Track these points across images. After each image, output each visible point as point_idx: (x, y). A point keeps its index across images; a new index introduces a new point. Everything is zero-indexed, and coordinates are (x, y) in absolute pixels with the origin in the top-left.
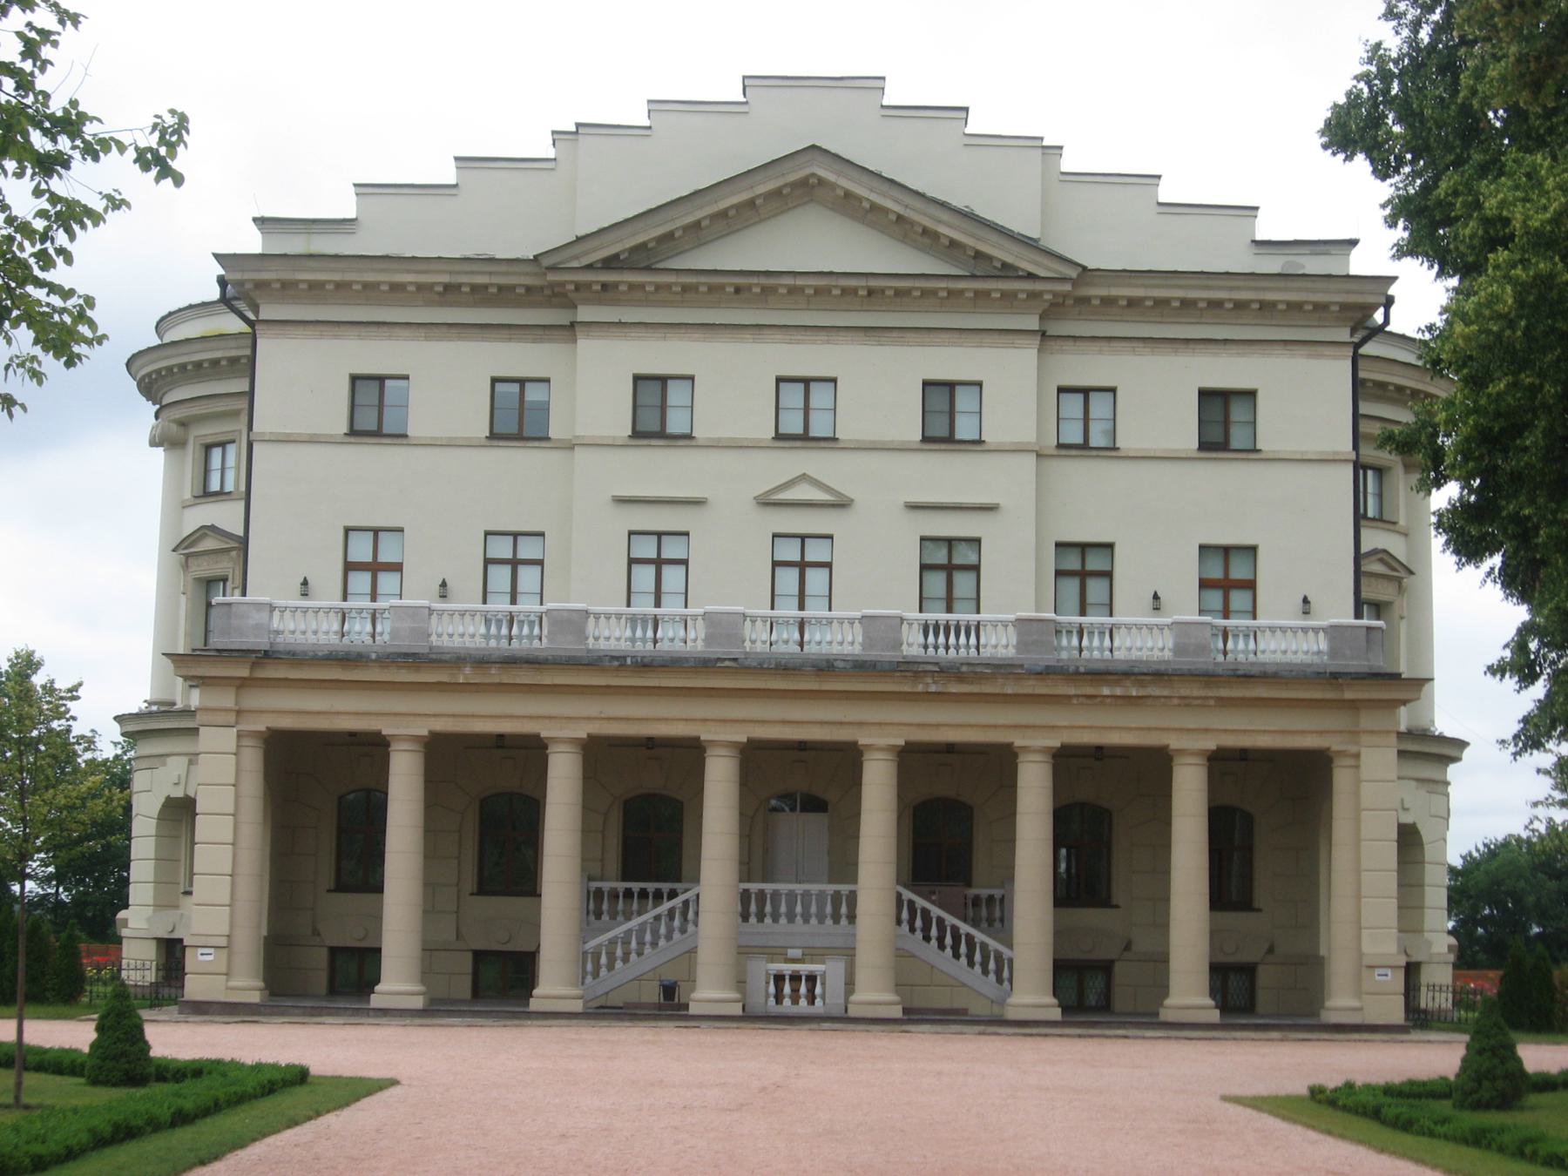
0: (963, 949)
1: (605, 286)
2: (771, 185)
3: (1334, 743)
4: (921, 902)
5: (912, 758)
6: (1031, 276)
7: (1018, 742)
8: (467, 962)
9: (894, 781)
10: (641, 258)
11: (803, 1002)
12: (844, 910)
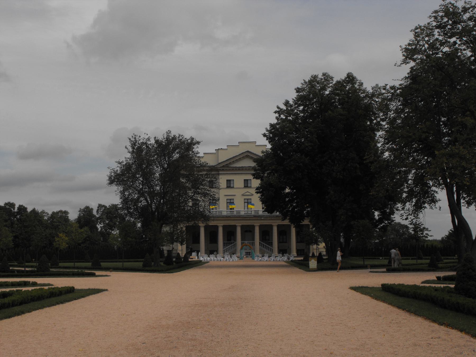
0: (268, 248)
1: (223, 169)
2: (243, 156)
4: (263, 243)
7: (273, 224)
10: (227, 166)
12: (254, 244)
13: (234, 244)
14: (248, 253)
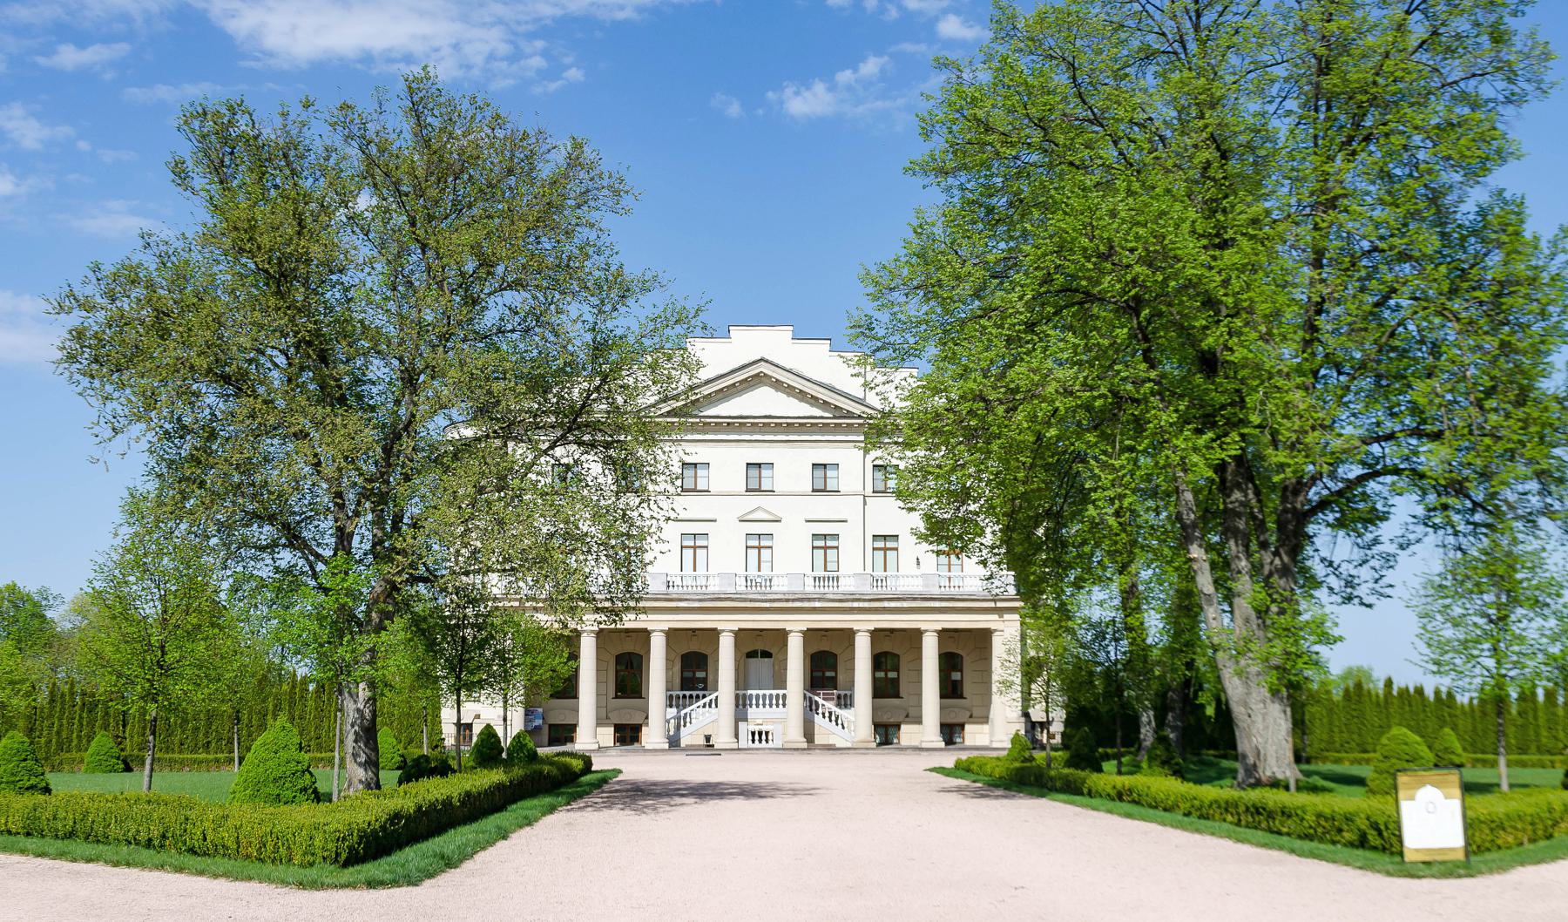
3: (992, 626)
13: (707, 700)
14: (760, 734)
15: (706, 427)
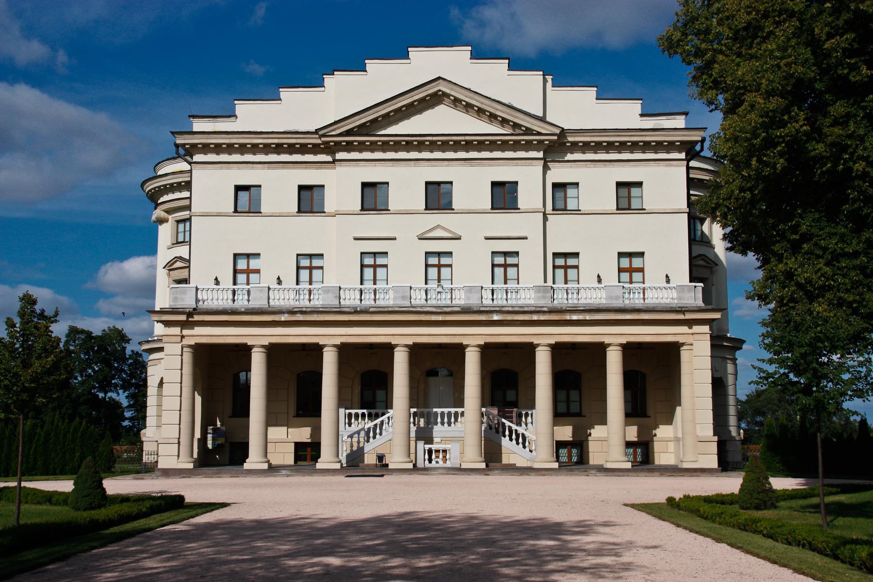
1: (348, 142)
3: (681, 339)
5: (488, 350)
6: (539, 134)
7: (535, 342)
8: (291, 448)
9: (480, 361)
10: (363, 129)
11: (441, 462)
13: (385, 418)
15: (385, 146)
